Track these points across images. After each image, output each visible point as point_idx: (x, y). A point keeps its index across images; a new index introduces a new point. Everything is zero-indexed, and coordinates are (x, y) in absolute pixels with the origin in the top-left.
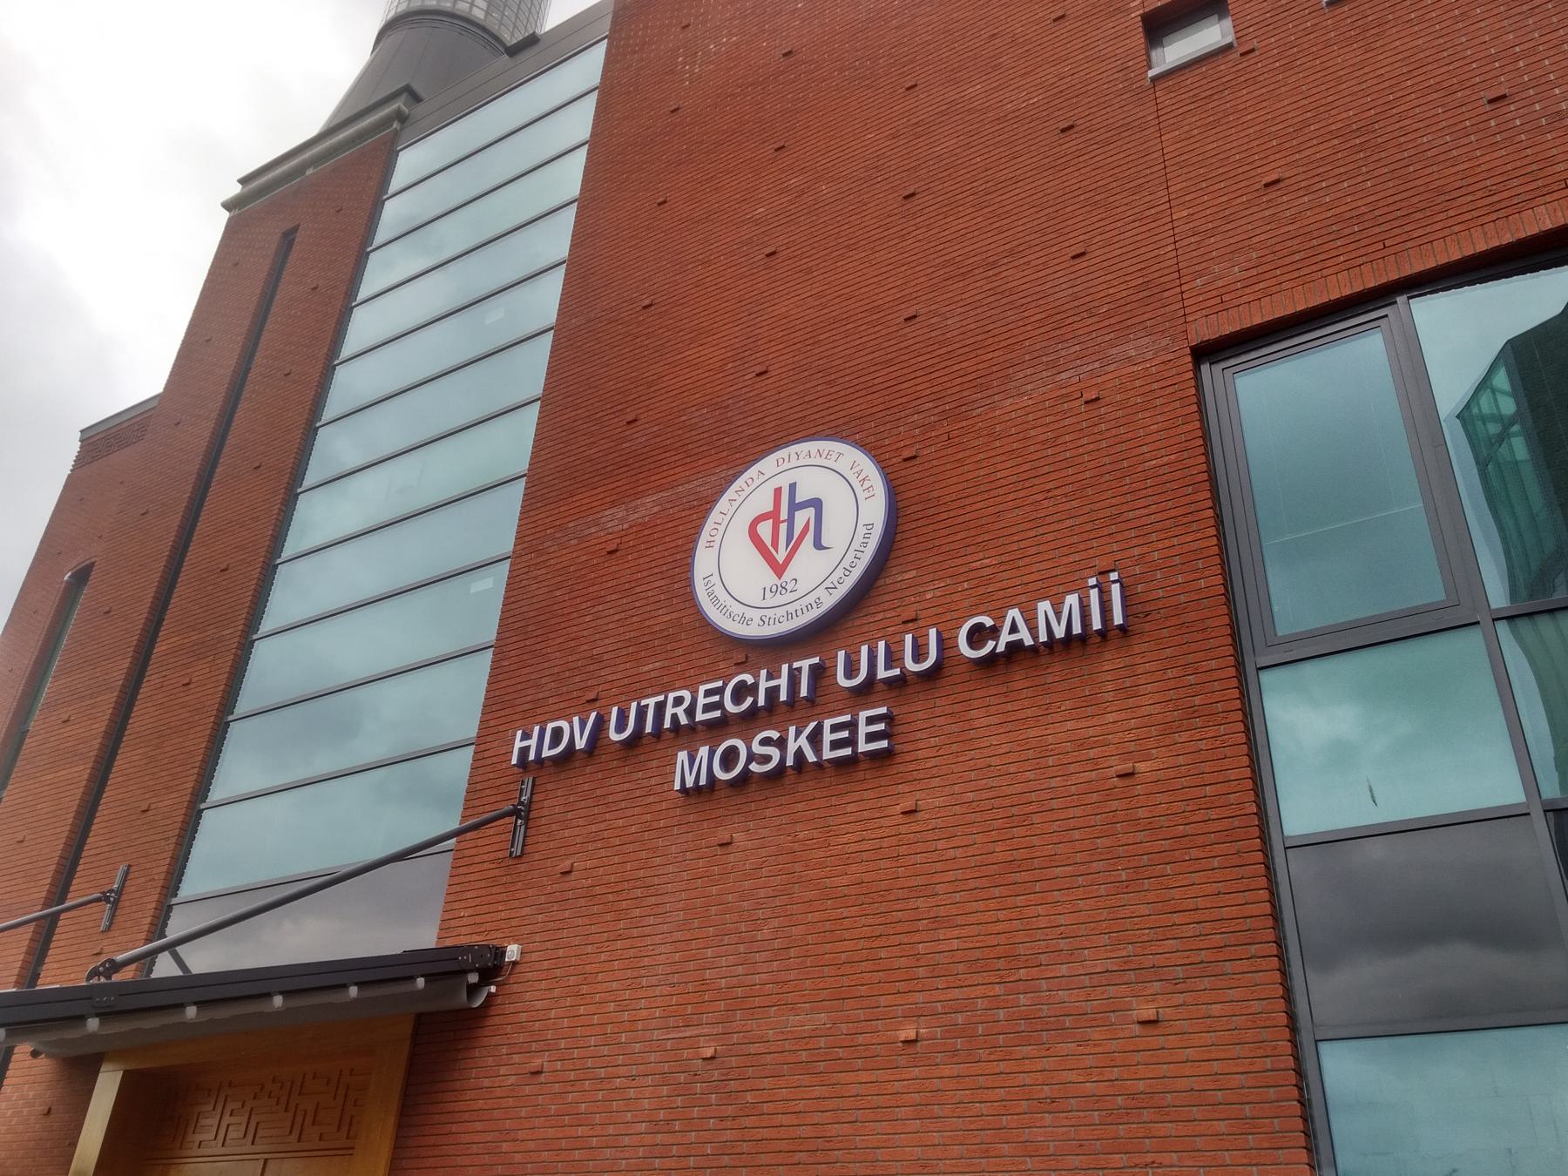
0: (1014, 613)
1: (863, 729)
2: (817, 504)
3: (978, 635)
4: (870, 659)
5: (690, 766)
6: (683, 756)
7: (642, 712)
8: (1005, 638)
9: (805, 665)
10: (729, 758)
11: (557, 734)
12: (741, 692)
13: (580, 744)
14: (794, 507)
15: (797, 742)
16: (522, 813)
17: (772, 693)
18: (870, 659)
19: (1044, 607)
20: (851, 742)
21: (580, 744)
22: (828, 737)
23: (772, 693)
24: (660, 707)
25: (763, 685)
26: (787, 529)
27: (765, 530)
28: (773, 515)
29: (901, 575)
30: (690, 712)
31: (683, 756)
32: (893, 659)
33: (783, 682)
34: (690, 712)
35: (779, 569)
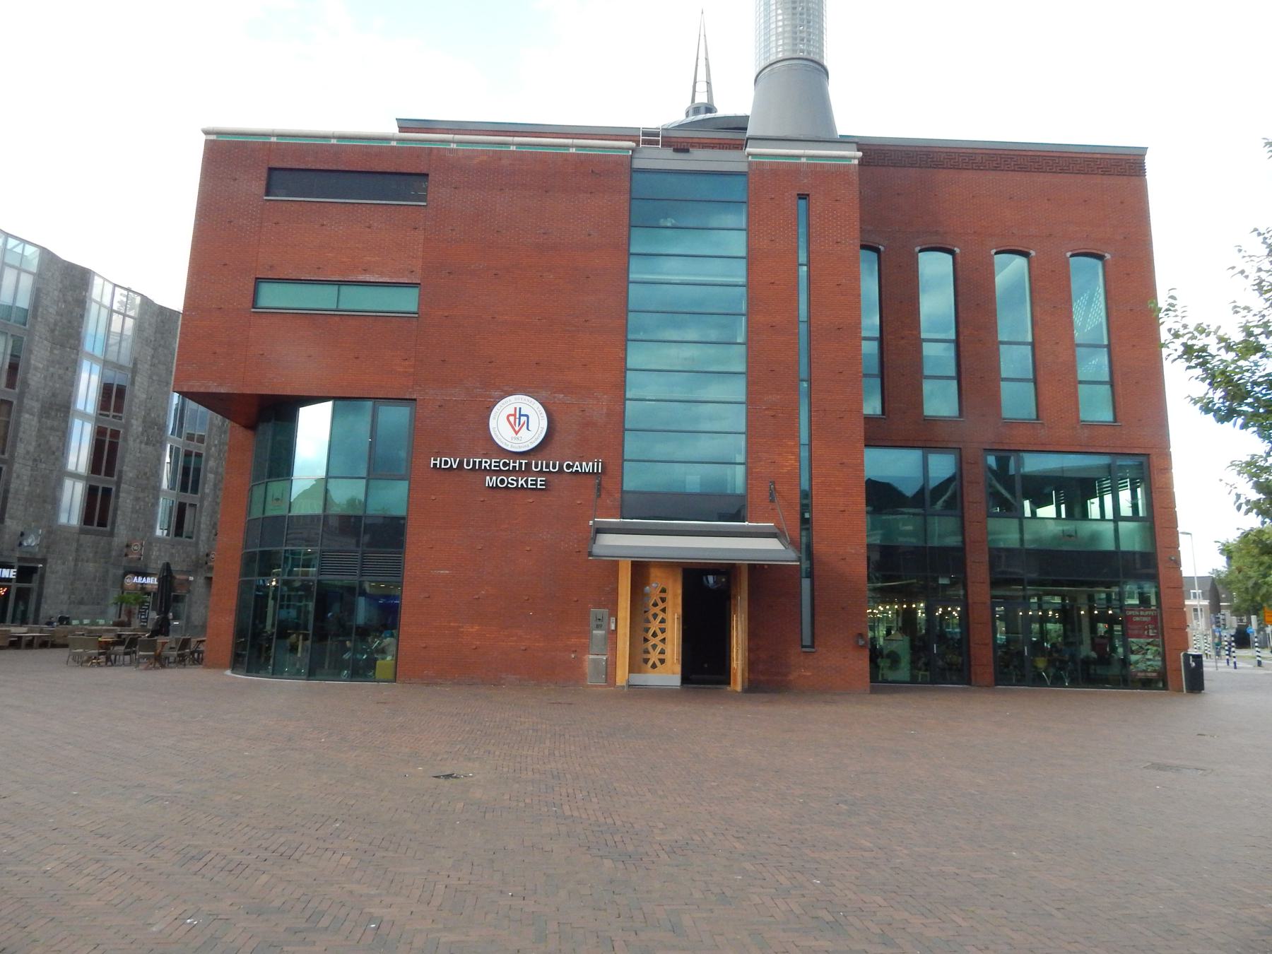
3: (569, 466)
5: (490, 481)
10: (502, 481)
11: (446, 462)
12: (505, 464)
18: (539, 464)
24: (480, 463)
26: (519, 421)
27: (512, 419)
32: (548, 466)
35: (517, 433)
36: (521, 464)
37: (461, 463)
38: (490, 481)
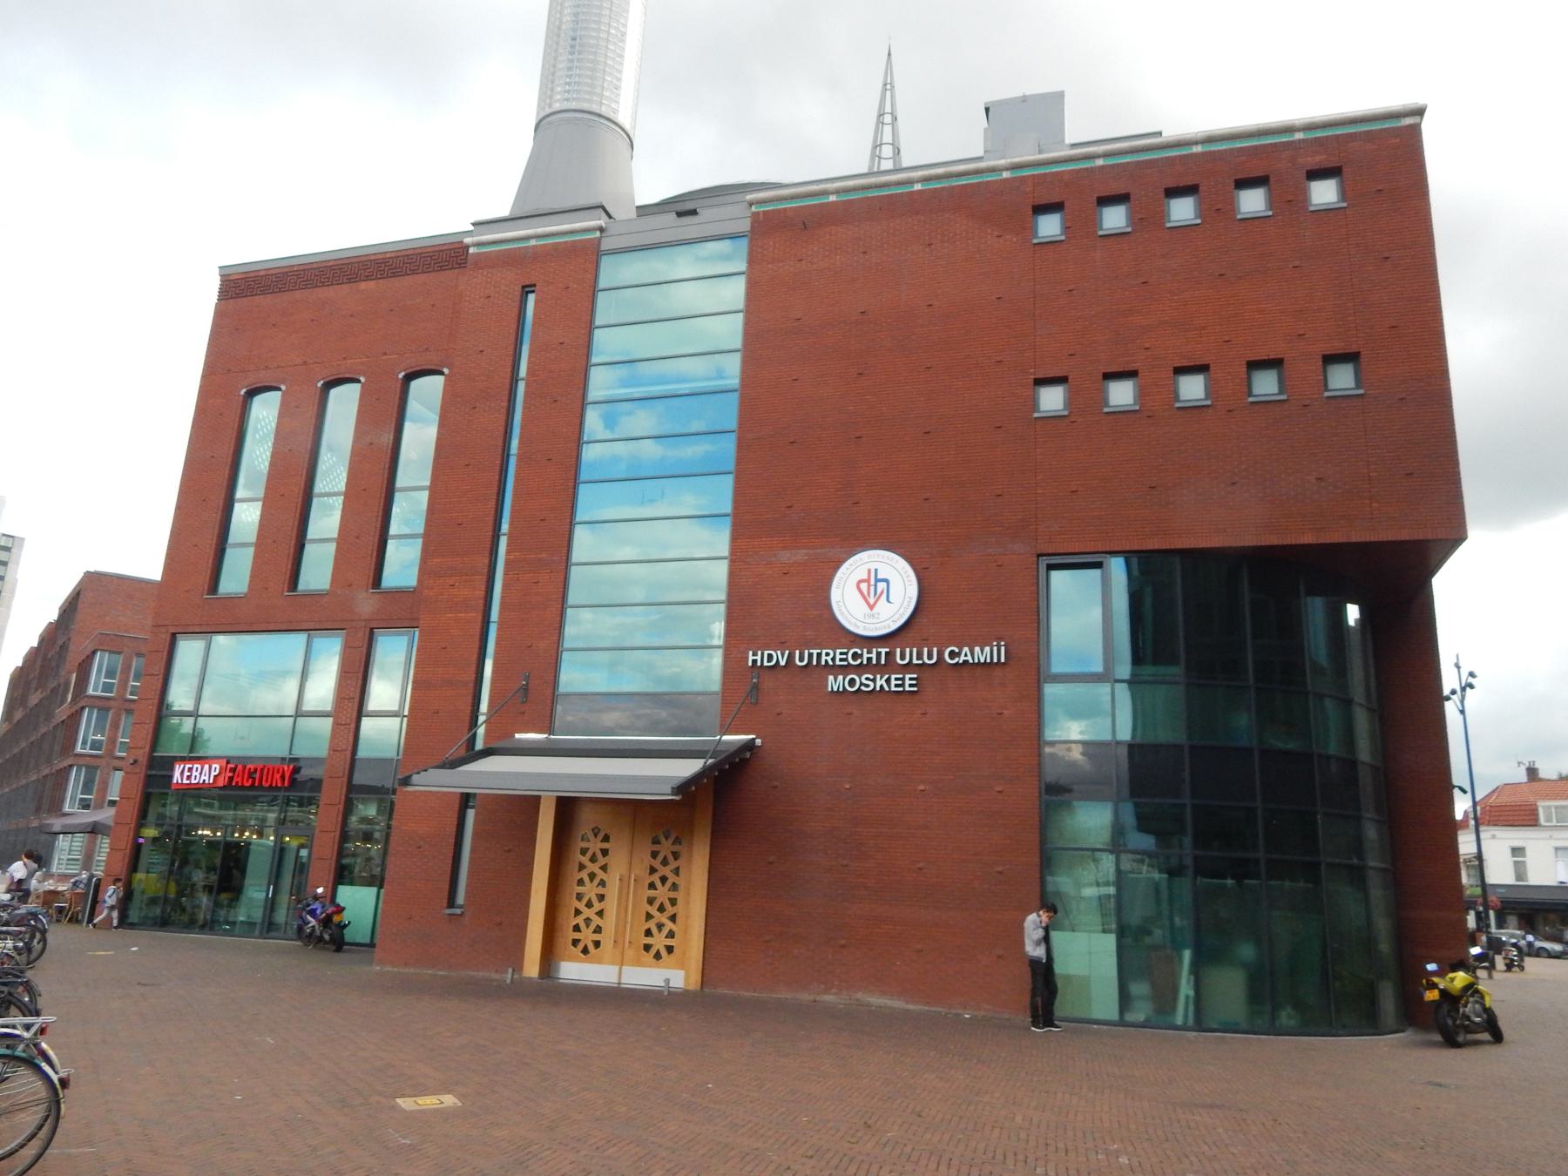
0: (966, 649)
1: (908, 682)
2: (886, 581)
3: (952, 655)
4: (910, 655)
5: (835, 683)
6: (831, 678)
7: (811, 655)
8: (963, 658)
9: (883, 651)
10: (852, 682)
11: (770, 657)
12: (855, 656)
13: (783, 663)
14: (877, 580)
15: (881, 682)
16: (756, 687)
17: (869, 659)
19: (977, 649)
20: (903, 685)
21: (783, 663)
22: (893, 682)
23: (869, 659)
24: (819, 655)
25: (866, 656)
26: (873, 588)
27: (864, 586)
28: (868, 581)
29: (922, 620)
30: (833, 659)
31: (831, 678)
32: (920, 656)
33: (874, 656)
34: (833, 659)
35: (871, 607)
36: (879, 654)
37: (791, 657)
38: (835, 683)
